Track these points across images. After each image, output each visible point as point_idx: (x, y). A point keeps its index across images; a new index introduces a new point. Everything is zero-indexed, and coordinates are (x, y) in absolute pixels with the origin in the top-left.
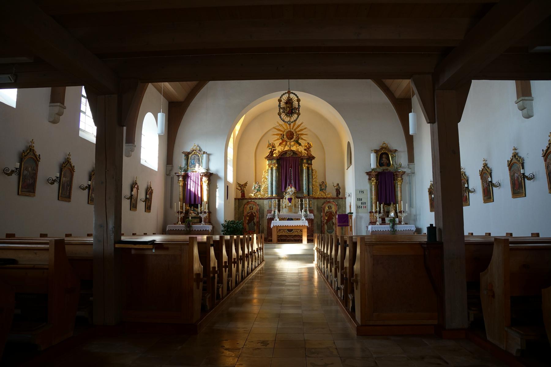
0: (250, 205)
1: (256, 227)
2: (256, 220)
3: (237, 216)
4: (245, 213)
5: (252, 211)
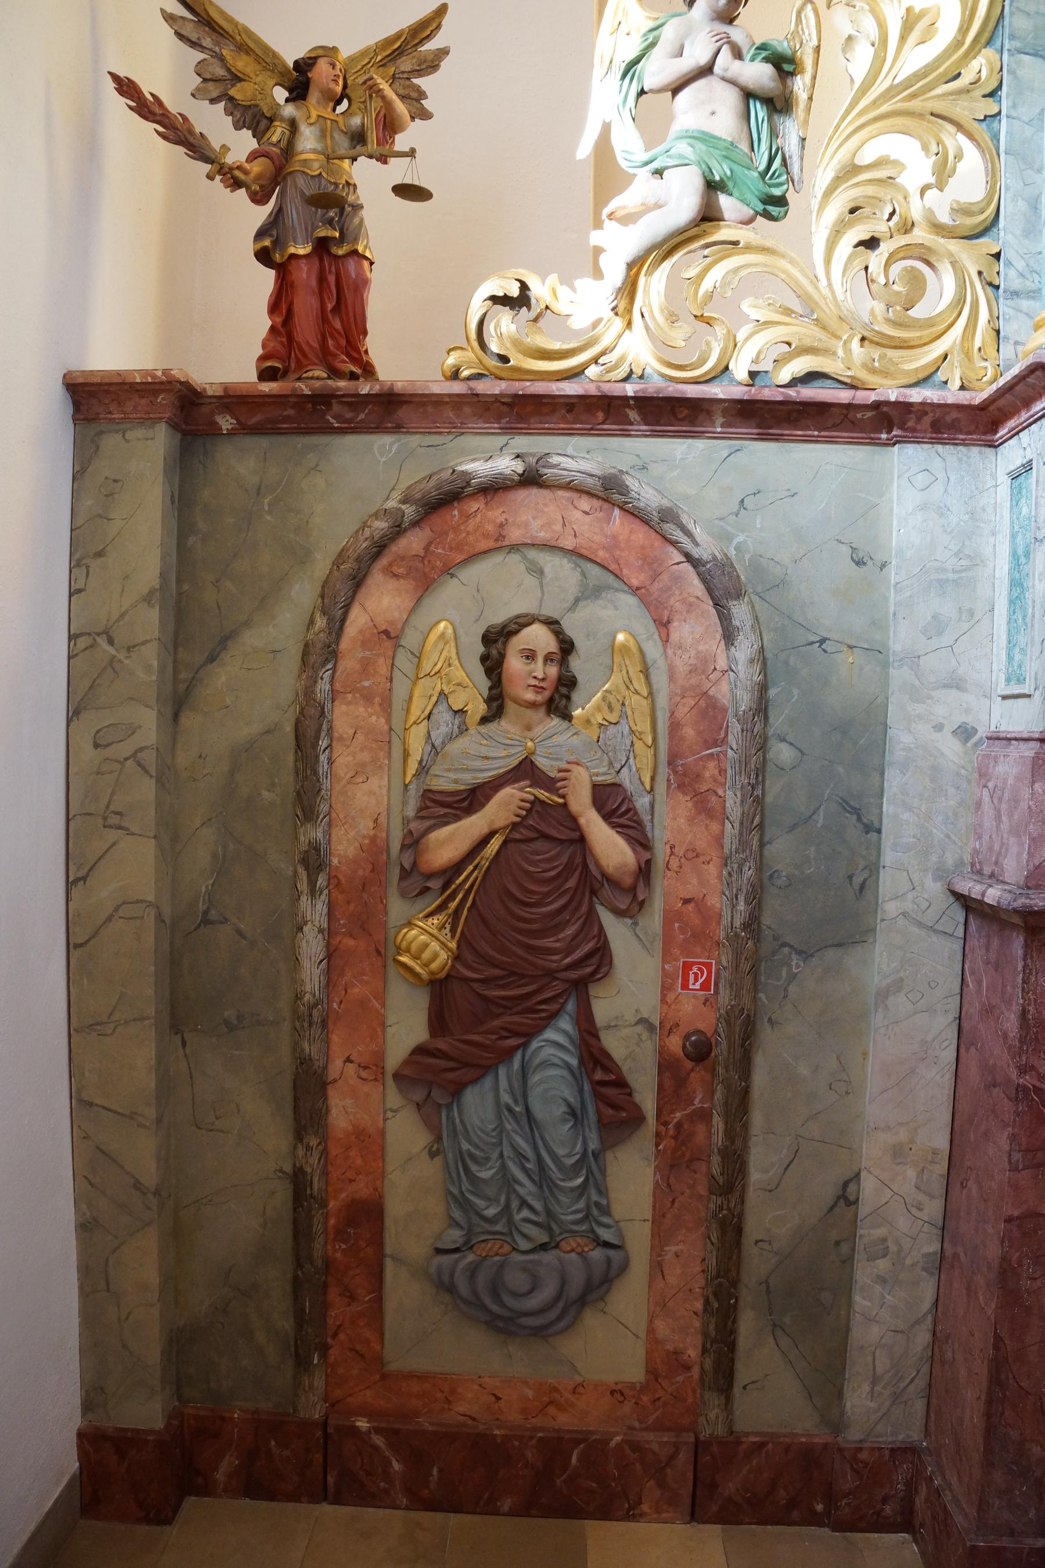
0: (498, 588)
1: (633, 1178)
2: (639, 992)
3: (135, 869)
4: (367, 802)
5: (553, 743)
